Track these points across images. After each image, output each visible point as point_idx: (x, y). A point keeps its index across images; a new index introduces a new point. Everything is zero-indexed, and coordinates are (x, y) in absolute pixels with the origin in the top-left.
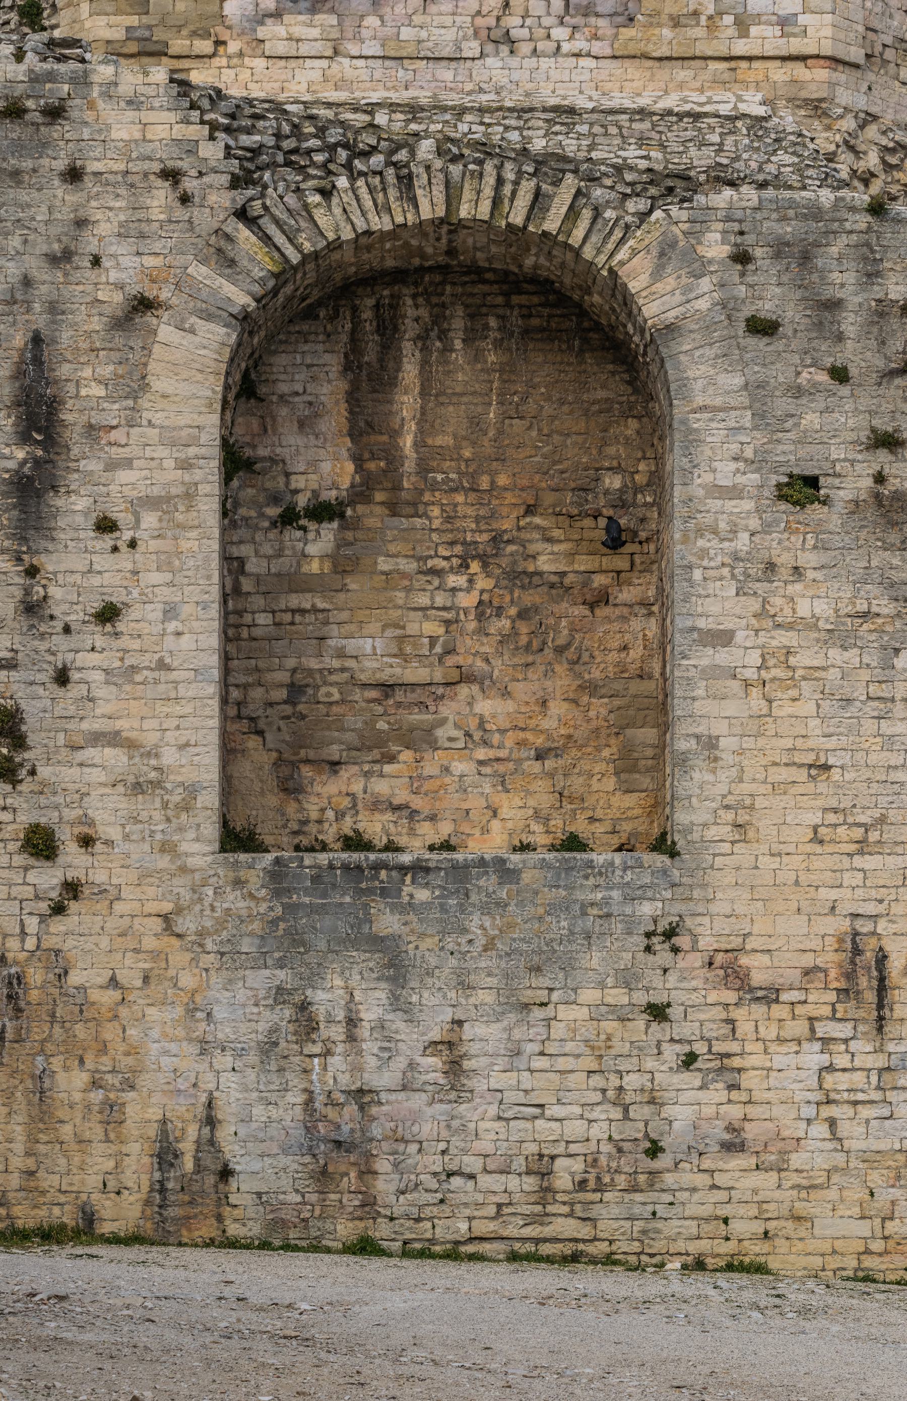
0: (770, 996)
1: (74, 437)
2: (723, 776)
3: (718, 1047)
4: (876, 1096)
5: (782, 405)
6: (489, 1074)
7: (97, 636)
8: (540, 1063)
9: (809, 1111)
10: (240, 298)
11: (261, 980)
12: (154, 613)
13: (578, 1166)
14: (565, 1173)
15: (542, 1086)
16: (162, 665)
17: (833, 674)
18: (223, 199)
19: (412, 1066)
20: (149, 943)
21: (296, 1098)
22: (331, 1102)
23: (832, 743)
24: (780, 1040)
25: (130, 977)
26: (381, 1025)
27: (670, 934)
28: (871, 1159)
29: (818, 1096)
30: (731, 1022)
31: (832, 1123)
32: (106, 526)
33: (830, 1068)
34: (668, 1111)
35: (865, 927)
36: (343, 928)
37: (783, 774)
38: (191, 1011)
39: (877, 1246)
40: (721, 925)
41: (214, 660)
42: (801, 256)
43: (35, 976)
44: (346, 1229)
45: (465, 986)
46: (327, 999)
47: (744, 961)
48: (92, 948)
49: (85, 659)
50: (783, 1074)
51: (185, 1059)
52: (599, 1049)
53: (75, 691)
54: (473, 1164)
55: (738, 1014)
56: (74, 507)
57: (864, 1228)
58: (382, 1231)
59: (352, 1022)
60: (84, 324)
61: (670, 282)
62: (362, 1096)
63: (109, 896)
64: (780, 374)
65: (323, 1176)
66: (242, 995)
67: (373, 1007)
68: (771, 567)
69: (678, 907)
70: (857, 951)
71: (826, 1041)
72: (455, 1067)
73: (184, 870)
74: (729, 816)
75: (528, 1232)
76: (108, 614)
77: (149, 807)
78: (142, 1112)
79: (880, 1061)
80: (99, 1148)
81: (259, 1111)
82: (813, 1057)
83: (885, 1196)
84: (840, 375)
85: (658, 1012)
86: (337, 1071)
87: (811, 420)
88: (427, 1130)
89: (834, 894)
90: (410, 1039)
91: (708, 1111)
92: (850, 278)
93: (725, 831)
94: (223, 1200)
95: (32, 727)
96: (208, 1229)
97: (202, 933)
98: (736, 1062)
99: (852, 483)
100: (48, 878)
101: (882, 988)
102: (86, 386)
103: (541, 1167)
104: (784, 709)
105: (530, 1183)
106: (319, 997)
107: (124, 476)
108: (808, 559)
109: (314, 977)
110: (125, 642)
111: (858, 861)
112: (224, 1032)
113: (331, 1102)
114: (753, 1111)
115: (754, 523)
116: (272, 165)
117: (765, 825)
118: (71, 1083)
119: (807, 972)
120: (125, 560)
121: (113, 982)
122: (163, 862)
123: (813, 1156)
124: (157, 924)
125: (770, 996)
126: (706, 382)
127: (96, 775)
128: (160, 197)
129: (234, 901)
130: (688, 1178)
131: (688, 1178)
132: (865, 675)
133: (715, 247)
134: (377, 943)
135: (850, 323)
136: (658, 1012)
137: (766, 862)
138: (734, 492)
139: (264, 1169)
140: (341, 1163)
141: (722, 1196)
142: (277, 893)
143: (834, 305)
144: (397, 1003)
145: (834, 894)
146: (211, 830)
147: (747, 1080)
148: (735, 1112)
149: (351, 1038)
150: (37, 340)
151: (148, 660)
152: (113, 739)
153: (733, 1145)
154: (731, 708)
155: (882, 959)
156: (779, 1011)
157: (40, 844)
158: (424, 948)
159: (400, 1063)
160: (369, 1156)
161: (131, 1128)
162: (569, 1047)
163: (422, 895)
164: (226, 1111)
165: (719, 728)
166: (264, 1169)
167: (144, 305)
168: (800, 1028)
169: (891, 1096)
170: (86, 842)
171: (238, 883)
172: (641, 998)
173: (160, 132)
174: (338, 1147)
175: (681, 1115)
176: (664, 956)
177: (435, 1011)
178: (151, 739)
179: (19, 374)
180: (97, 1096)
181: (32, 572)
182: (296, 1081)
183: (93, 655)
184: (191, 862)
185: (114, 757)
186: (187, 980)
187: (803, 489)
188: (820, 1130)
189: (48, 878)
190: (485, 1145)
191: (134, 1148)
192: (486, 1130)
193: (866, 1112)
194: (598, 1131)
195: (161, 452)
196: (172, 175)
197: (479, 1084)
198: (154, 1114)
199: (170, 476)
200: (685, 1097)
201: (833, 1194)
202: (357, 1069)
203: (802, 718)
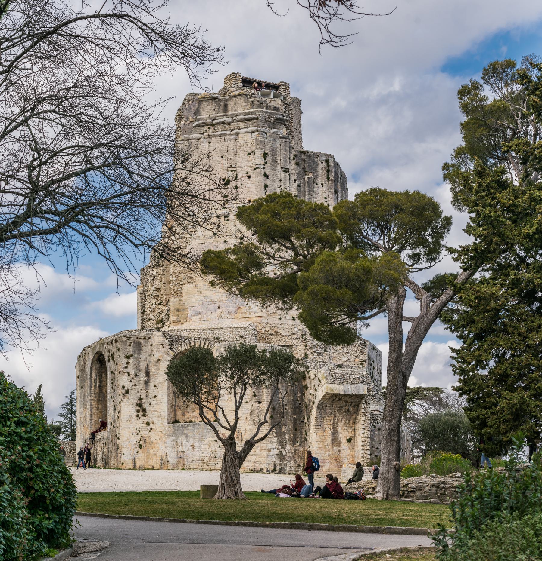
6: (197, 448)
7: (154, 399)
11: (172, 439)
14: (206, 460)
15: (203, 450)
25: (158, 439)
32: (155, 386)
43: (147, 439)
44: (181, 468)
46: (179, 441)
52: (209, 445)
56: (151, 384)
58: (185, 468)
60: (152, 363)
67: (184, 441)
72: (193, 448)
76: (155, 397)
77: (160, 419)
78: (159, 455)
86: (180, 449)
95: (147, 410)
100: (149, 428)
103: (203, 460)
118: (151, 451)
128: (161, 346)
129: (169, 429)
134: (185, 434)
139: (173, 461)
140: (181, 460)
144: (187, 441)
152: (156, 411)
157: (148, 424)
158: (190, 434)
174: (180, 458)
183: (154, 401)
185: (156, 413)
189: (149, 428)
192: (197, 456)
196: (162, 345)
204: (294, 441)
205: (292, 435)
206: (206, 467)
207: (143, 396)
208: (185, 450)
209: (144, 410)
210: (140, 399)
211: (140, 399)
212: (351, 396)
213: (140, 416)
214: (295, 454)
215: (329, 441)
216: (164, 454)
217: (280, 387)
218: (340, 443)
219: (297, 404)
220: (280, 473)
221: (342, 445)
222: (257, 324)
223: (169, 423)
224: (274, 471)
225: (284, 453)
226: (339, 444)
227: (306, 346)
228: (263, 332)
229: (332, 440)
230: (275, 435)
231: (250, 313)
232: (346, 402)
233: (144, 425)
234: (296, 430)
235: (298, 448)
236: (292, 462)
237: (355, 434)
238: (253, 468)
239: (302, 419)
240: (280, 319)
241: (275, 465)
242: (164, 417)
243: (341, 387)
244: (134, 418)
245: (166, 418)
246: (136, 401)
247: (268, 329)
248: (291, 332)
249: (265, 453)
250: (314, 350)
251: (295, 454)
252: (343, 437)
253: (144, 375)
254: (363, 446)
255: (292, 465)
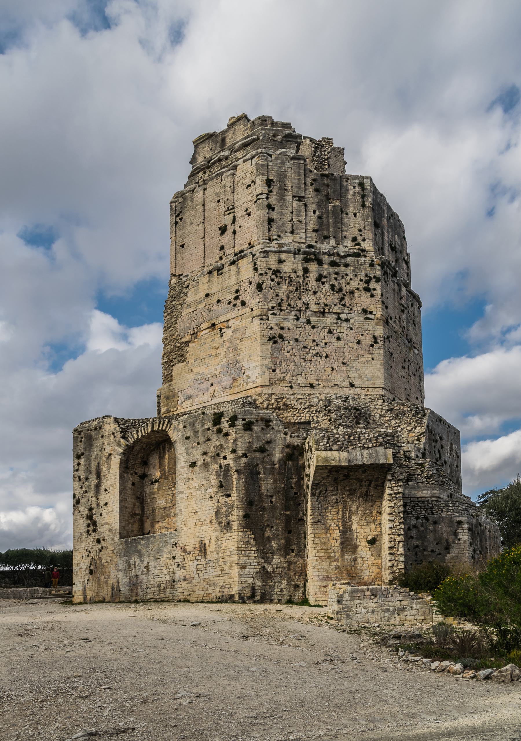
0: (189, 553)
1: (102, 477)
2: (183, 516)
3: (183, 563)
4: (204, 569)
5: (190, 451)
6: (152, 571)
7: (105, 508)
8: (159, 568)
9: (195, 572)
10: (121, 450)
11: (124, 559)
12: (111, 503)
13: (164, 585)
14: (163, 586)
16: (112, 511)
17: (198, 496)
18: (119, 436)
19: (143, 571)
20: (111, 555)
21: (128, 578)
22: (133, 578)
23: (198, 508)
24: (191, 561)
25: (109, 561)
26: (139, 564)
27: (176, 544)
28: (204, 580)
29: (196, 570)
30: (184, 558)
31: (198, 574)
32: (106, 490)
33: (198, 565)
34: (176, 575)
35: (203, 539)
36: (134, 549)
37: (191, 514)
38: (116, 565)
39: (205, 595)
40: (183, 542)
41: (118, 509)
42: (193, 424)
43: (98, 562)
44: (134, 598)
45: (149, 557)
47: (186, 547)
48: (105, 557)
49: (104, 511)
50: (191, 566)
51: (116, 574)
53: (103, 516)
54: (150, 586)
55: (185, 557)
56: (102, 488)
57: (203, 592)
58: (139, 599)
59: (135, 564)
61: (175, 434)
62: (137, 576)
63: (106, 548)
64: (190, 446)
65: (132, 590)
66: (122, 561)
68: (189, 479)
69: (177, 540)
70: (202, 544)
71: (197, 560)
72: (148, 571)
73: (115, 543)
74: (183, 523)
75: (157, 597)
76: (106, 504)
77: (111, 533)
78: (110, 582)
79: (205, 562)
80: (105, 588)
81: (124, 580)
82: (196, 563)
83: (206, 586)
84: (198, 443)
85: (174, 558)
86: (133, 573)
87: (194, 452)
88: (144, 581)
89: (198, 534)
90: (142, 566)
91: (181, 574)
92: (200, 426)
93: (183, 526)
94: (120, 595)
96: (117, 600)
97: (117, 552)
98: (185, 565)
99: (200, 462)
100: (99, 546)
101: (205, 550)
102: (104, 468)
103: (159, 586)
104: (191, 503)
105: (157, 589)
106: (131, 561)
107: (108, 482)
108: (194, 476)
109: (130, 558)
110: (108, 508)
111: (202, 528)
112: (120, 568)
113: (133, 578)
114: (188, 573)
115: (187, 472)
116: (130, 428)
117: (188, 524)
119: (194, 548)
120: (108, 495)
121: (107, 562)
122: (113, 542)
123: (196, 581)
124: (112, 552)
125: (189, 553)
126: (180, 449)
127: (105, 529)
129: (121, 547)
130: (179, 586)
131: (179, 586)
132: (202, 495)
133: (181, 426)
135: (200, 434)
136: (174, 558)
137: (189, 530)
138: (184, 467)
139: (124, 589)
140: (134, 587)
141: (183, 588)
142: (126, 545)
143: (197, 432)
144: (141, 561)
145: (198, 534)
146: (118, 536)
147: (186, 568)
148: (184, 574)
149: (135, 567)
150: (98, 463)
151: (110, 510)
153: (185, 580)
154: (184, 504)
155: (205, 544)
156: (191, 555)
158: (144, 552)
159: (141, 570)
160: (137, 586)
161: (109, 585)
162: (163, 565)
163: (144, 542)
164: (120, 581)
165: (182, 508)
166: (124, 589)
167: (110, 455)
168: (194, 558)
169: (207, 568)
170: (104, 540)
171: (121, 544)
172: (172, 556)
173: (112, 427)
174: (134, 584)
175: (177, 575)
176: (175, 548)
177: (145, 560)
178: (111, 523)
179: (96, 469)
180: (105, 580)
181: (98, 499)
182: (128, 575)
184: (116, 541)
185: (107, 526)
186: (115, 560)
187: (193, 465)
188: (197, 576)
190: (152, 583)
191: (109, 588)
193: (203, 572)
194: (166, 579)
195: (112, 477)
197: (151, 573)
198: (112, 582)
199: (113, 481)
200: (178, 572)
201: (198, 587)
202: (136, 572)
203: (194, 504)
204: (286, 550)
205: (283, 541)
206: (162, 596)
207: (94, 505)
208: (139, 573)
209: (95, 524)
210: (91, 509)
211: (91, 509)
212: (364, 468)
213: (91, 532)
214: (289, 569)
215: (336, 545)
216: (115, 580)
217: (262, 471)
218: (356, 547)
219: (291, 493)
220: (262, 601)
221: (359, 549)
222: (257, 397)
223: (121, 538)
224: (253, 596)
225: (270, 569)
226: (354, 549)
227: (330, 420)
228: (265, 405)
229: (342, 543)
230: (253, 543)
231: (247, 384)
232: (360, 481)
233: (95, 543)
234: (290, 532)
235: (294, 559)
236: (285, 581)
237: (381, 532)
238: (220, 594)
239: (301, 515)
240: (291, 387)
241: (253, 589)
242: (116, 530)
243: (344, 455)
244: (85, 534)
245: (118, 531)
246: (86, 513)
247: (273, 401)
248: (308, 404)
249: (235, 571)
250: (338, 422)
251: (289, 569)
252: (361, 537)
253: (94, 477)
254: (390, 548)
255: (283, 586)
